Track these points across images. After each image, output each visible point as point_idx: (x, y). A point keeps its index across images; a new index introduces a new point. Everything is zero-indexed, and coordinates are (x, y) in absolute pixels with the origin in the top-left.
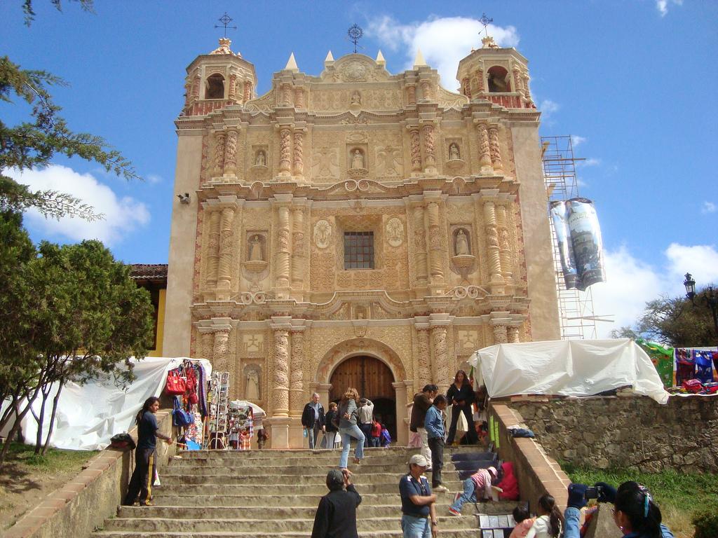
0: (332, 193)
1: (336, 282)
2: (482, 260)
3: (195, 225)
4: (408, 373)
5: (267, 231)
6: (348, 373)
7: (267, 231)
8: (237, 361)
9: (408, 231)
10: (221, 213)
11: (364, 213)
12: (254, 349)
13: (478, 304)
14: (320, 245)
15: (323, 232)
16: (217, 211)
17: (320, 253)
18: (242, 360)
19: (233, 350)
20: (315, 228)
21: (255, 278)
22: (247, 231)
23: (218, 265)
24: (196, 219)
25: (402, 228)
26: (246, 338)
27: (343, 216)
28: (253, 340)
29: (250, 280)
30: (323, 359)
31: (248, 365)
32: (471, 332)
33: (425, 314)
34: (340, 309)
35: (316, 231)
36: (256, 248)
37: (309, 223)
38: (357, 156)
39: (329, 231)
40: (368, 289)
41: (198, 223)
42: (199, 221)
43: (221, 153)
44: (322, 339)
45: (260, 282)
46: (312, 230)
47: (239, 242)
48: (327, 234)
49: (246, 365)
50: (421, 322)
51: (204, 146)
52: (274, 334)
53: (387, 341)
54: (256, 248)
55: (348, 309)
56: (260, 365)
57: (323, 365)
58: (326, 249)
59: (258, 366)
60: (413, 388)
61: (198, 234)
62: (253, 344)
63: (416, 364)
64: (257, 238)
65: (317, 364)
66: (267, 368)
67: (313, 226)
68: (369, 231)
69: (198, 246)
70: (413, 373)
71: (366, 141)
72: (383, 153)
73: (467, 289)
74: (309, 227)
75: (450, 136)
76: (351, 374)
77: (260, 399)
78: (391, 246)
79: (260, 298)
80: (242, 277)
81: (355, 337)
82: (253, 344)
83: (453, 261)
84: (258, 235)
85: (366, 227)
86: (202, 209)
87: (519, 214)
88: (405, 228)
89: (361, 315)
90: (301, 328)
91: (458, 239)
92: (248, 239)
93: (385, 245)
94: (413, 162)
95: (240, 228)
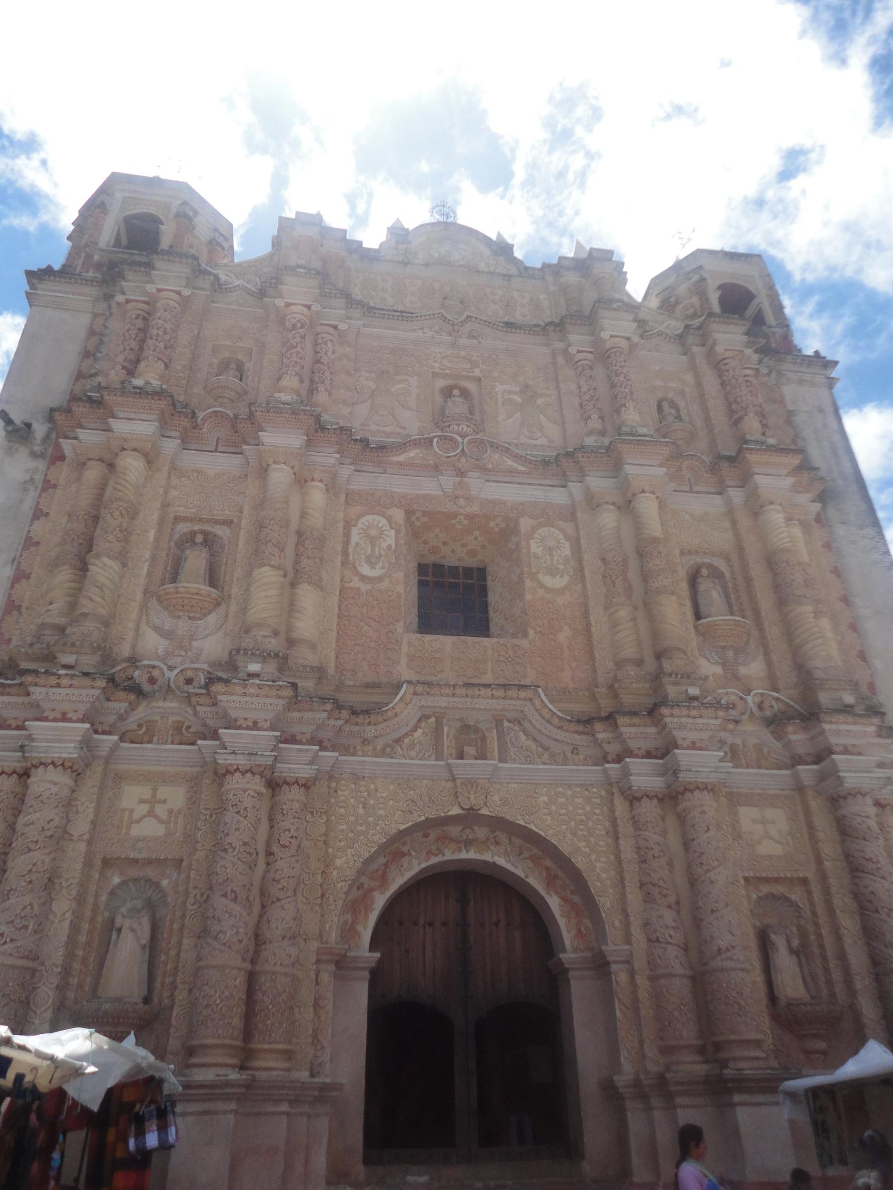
0: (401, 458)
1: (404, 661)
2: (773, 632)
3: (33, 494)
4: (613, 923)
5: (228, 523)
6: (422, 922)
7: (228, 523)
8: (88, 864)
9: (586, 557)
10: (111, 466)
11: (475, 509)
12: (150, 829)
13: (779, 738)
14: (366, 570)
15: (373, 540)
16: (100, 460)
17: (364, 588)
18: (107, 863)
19: (81, 827)
20: (355, 531)
21: (182, 627)
22: (178, 519)
23: (80, 590)
24: (39, 478)
25: (566, 550)
26: (132, 796)
27: (424, 513)
28: (153, 801)
29: (167, 635)
30: (361, 873)
31: (124, 883)
32: (770, 813)
33: (648, 755)
34: (414, 730)
35: (355, 536)
36: (196, 561)
37: (341, 515)
38: (456, 398)
39: (391, 541)
40: (488, 678)
41: (44, 490)
42: (48, 485)
43: (134, 345)
44: (361, 811)
45: (195, 644)
46: (347, 535)
47: (151, 535)
48: (384, 545)
49: (116, 880)
50: (644, 775)
51: (92, 332)
52: (221, 785)
53: (544, 825)
54: (196, 561)
55: (438, 731)
56: (165, 883)
57: (355, 893)
58: (380, 579)
59: (157, 886)
60: (632, 974)
61: (38, 513)
62: (151, 813)
63: (634, 897)
64: (199, 538)
65: (343, 886)
66: (186, 890)
67: (348, 525)
68: (474, 566)
69: (30, 543)
70: (627, 924)
71: (477, 372)
72: (518, 399)
73: (749, 699)
74: (341, 525)
75: (659, 383)
76: (430, 924)
77: (147, 1000)
78: (541, 585)
79: (189, 681)
80: (144, 626)
81: (455, 811)
82: (151, 813)
83: (696, 627)
84: (204, 533)
85: (472, 553)
86: (62, 458)
87: (828, 546)
88: (577, 548)
89: (471, 750)
90: (304, 772)
91: (702, 587)
92: (176, 537)
93: (528, 583)
94: (587, 419)
95: (158, 504)
